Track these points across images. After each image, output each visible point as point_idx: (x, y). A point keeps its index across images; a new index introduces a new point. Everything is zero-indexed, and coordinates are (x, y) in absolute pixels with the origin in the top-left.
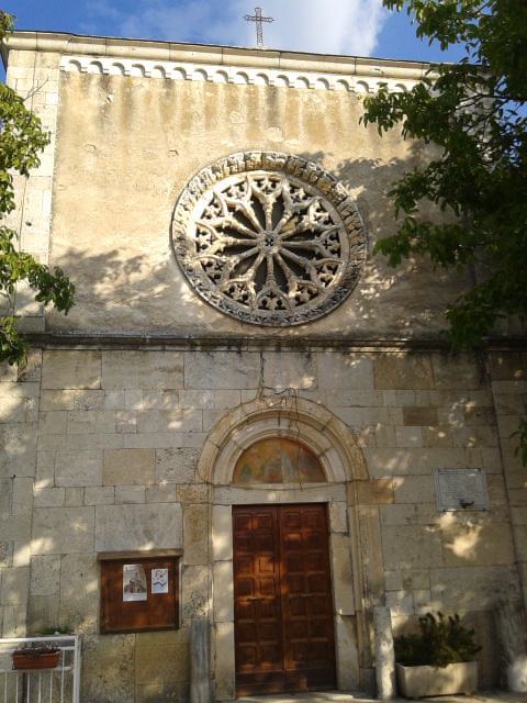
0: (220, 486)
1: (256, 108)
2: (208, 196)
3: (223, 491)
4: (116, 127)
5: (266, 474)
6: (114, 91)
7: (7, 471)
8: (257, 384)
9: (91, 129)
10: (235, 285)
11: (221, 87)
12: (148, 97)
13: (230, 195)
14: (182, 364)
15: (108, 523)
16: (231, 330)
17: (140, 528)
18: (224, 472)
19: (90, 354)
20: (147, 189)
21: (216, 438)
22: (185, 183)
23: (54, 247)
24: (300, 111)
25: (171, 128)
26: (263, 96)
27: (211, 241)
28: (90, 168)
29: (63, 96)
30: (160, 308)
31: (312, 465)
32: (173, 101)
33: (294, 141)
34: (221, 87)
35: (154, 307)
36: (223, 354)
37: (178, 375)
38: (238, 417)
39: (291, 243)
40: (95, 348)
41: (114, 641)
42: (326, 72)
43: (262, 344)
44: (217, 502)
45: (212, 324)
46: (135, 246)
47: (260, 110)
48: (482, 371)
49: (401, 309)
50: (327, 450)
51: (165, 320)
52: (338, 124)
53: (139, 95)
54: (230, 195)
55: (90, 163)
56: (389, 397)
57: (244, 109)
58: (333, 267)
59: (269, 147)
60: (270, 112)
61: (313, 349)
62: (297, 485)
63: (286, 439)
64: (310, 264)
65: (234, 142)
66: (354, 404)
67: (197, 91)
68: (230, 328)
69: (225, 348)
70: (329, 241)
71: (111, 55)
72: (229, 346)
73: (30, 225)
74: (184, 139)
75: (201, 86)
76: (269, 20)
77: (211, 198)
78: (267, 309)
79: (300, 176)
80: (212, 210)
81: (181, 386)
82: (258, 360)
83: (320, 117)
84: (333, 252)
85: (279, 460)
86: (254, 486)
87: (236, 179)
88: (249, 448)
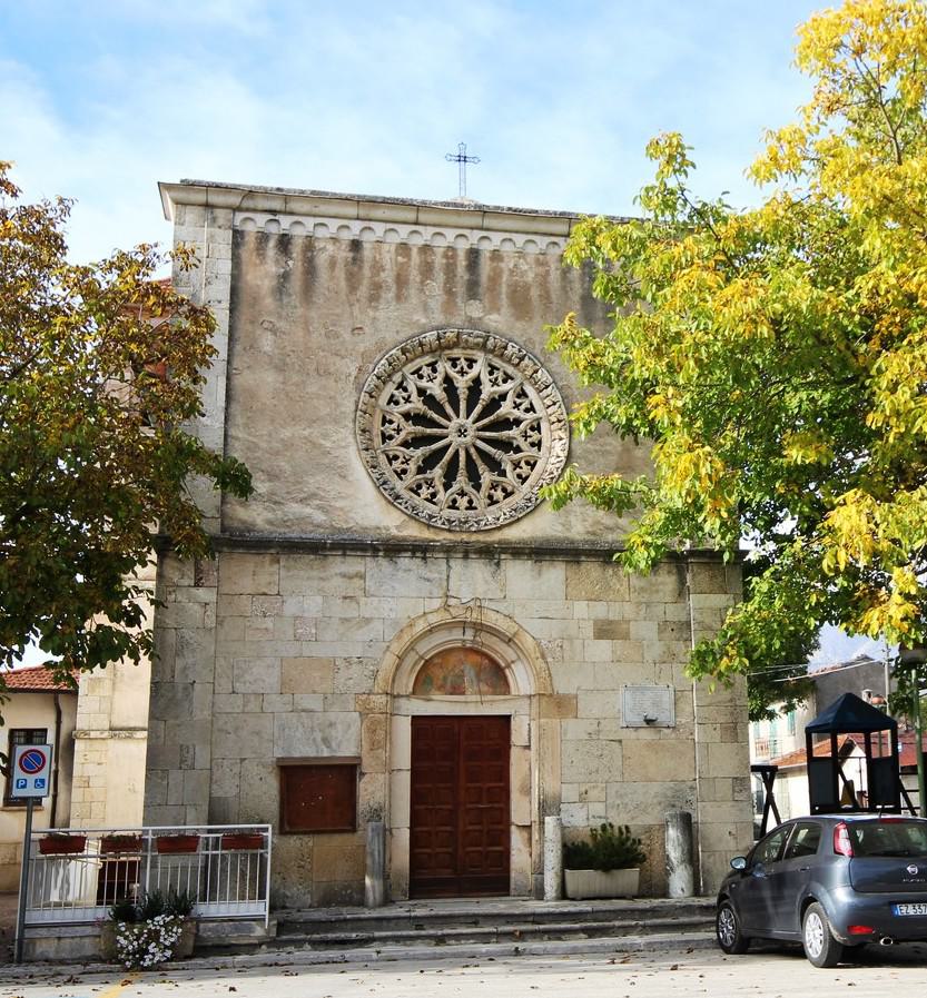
1: (455, 276)
2: (397, 378)
3: (403, 701)
4: (295, 299)
5: (449, 684)
6: (294, 255)
7: (187, 676)
8: (441, 593)
9: (269, 301)
10: (422, 481)
12: (333, 263)
13: (421, 377)
14: (363, 570)
15: (287, 730)
16: (415, 534)
17: (319, 736)
18: (405, 682)
19: (268, 558)
21: (397, 648)
22: (371, 366)
23: (229, 439)
24: (504, 279)
25: (358, 300)
27: (398, 431)
28: (267, 348)
30: (342, 509)
31: (497, 677)
32: (361, 268)
33: (494, 317)
35: (336, 508)
36: (407, 560)
37: (358, 582)
38: (421, 626)
39: (488, 434)
40: (273, 551)
41: (292, 841)
42: (536, 233)
43: (448, 550)
44: (396, 712)
45: (397, 527)
46: (315, 440)
48: (682, 581)
50: (513, 662)
51: (346, 522)
52: (546, 296)
53: (322, 260)
55: (267, 342)
56: (581, 609)
57: (440, 277)
59: (467, 324)
60: (468, 280)
61: (503, 556)
62: (478, 698)
63: (473, 651)
64: (506, 459)
66: (542, 615)
67: (388, 258)
68: (414, 532)
69: (409, 554)
70: (530, 433)
72: (414, 552)
74: (371, 313)
75: (393, 248)
76: (476, 160)
77: (400, 380)
78: (458, 509)
79: (501, 356)
80: (399, 394)
81: (361, 593)
82: (444, 567)
83: (527, 287)
84: (533, 445)
86: (434, 697)
87: (428, 359)
88: (430, 659)
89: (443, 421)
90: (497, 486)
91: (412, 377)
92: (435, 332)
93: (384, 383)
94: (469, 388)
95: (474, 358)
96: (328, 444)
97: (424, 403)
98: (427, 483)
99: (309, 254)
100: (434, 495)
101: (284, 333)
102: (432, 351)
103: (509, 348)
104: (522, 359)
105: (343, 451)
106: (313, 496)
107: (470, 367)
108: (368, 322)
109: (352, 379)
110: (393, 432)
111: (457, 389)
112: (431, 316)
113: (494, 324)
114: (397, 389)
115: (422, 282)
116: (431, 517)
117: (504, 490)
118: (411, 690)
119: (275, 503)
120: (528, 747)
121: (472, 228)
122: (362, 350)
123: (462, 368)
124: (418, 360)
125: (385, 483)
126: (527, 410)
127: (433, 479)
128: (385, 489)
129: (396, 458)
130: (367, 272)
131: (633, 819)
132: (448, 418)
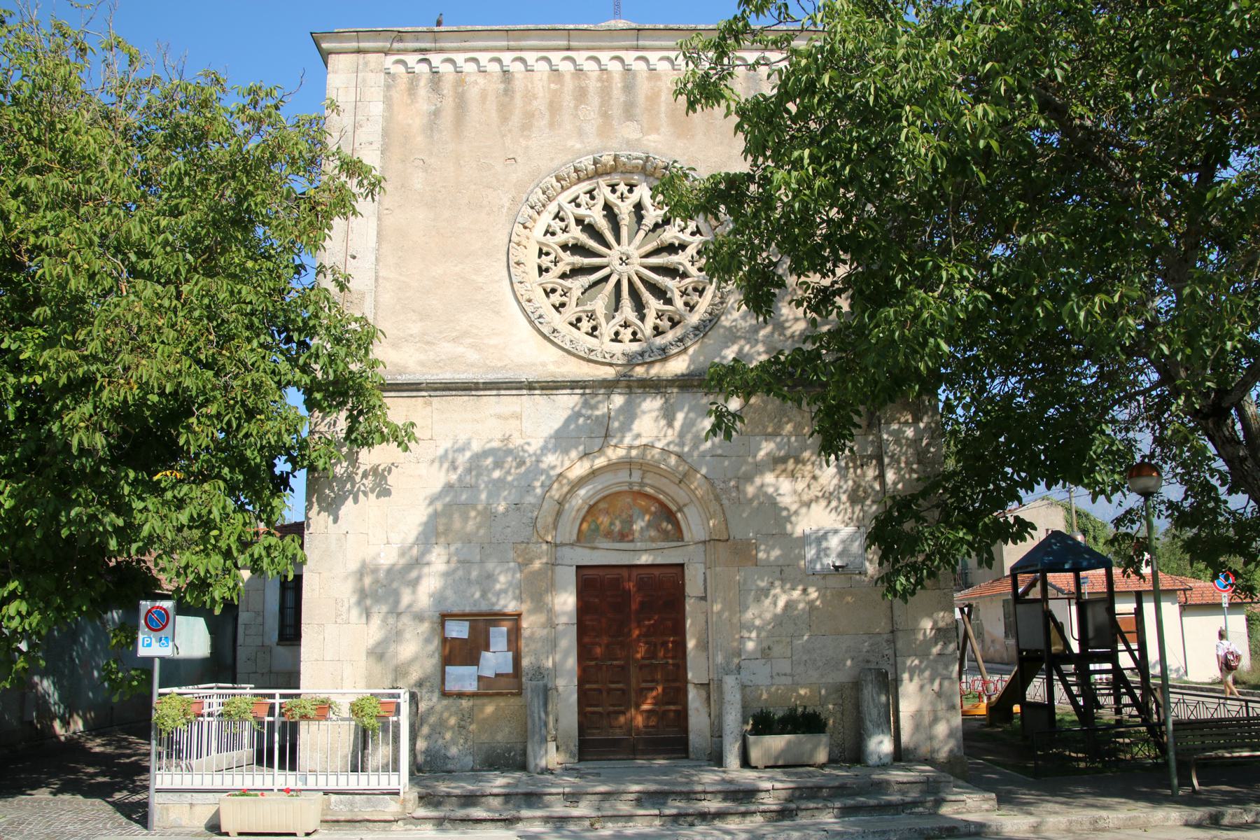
0: (563, 545)
2: (553, 208)
3: (566, 550)
6: (445, 92)
9: (420, 139)
11: (568, 78)
12: (484, 96)
13: (578, 206)
23: (380, 281)
25: (510, 131)
26: (617, 83)
27: (556, 263)
28: (418, 186)
29: (388, 101)
32: (512, 98)
33: (653, 137)
34: (568, 78)
37: (514, 423)
45: (556, 363)
47: (614, 101)
50: (685, 505)
53: (473, 93)
54: (578, 206)
55: (418, 181)
57: (595, 101)
69: (568, 391)
71: (441, 50)
73: (354, 257)
74: (523, 142)
75: (545, 77)
77: (556, 210)
78: (620, 341)
80: (556, 225)
85: (631, 516)
86: (601, 545)
88: (596, 504)
93: (539, 213)
95: (633, 182)
99: (460, 89)
100: (594, 328)
101: (435, 169)
102: (589, 178)
106: (465, 334)
107: (631, 191)
109: (505, 210)
115: (576, 107)
118: (574, 537)
119: (428, 343)
120: (704, 598)
121: (627, 49)
124: (575, 188)
125: (540, 317)
126: (693, 234)
127: (593, 312)
130: (518, 101)
131: (822, 676)
132: (608, 246)
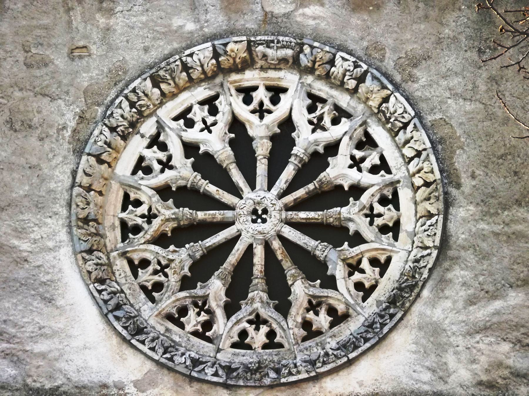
10: (188, 302)
20: (30, 127)
27: (150, 217)
30: (43, 355)
39: (303, 215)
49: (506, 347)
51: (51, 377)
54: (190, 124)
58: (383, 259)
65: (197, 20)
70: (378, 208)
74: (102, 20)
77: (153, 131)
78: (249, 347)
79: (327, 77)
84: (384, 229)
89: (227, 198)
90: (319, 304)
91: (174, 124)
92: (209, 44)
94: (273, 138)
95: (283, 84)
96: (25, 246)
97: (195, 167)
98: (196, 305)
100: (208, 325)
103: (338, 61)
104: (361, 79)
105: (49, 257)
107: (275, 101)
108: (96, 36)
109: (68, 134)
110: (139, 221)
111: (252, 139)
112: (203, 18)
113: (311, 22)
114: (149, 146)
116: (196, 362)
117: (332, 311)
122: (86, 84)
123: (261, 104)
125: (118, 307)
127: (205, 299)
128: (117, 318)
129: (145, 263)
132: (236, 192)
